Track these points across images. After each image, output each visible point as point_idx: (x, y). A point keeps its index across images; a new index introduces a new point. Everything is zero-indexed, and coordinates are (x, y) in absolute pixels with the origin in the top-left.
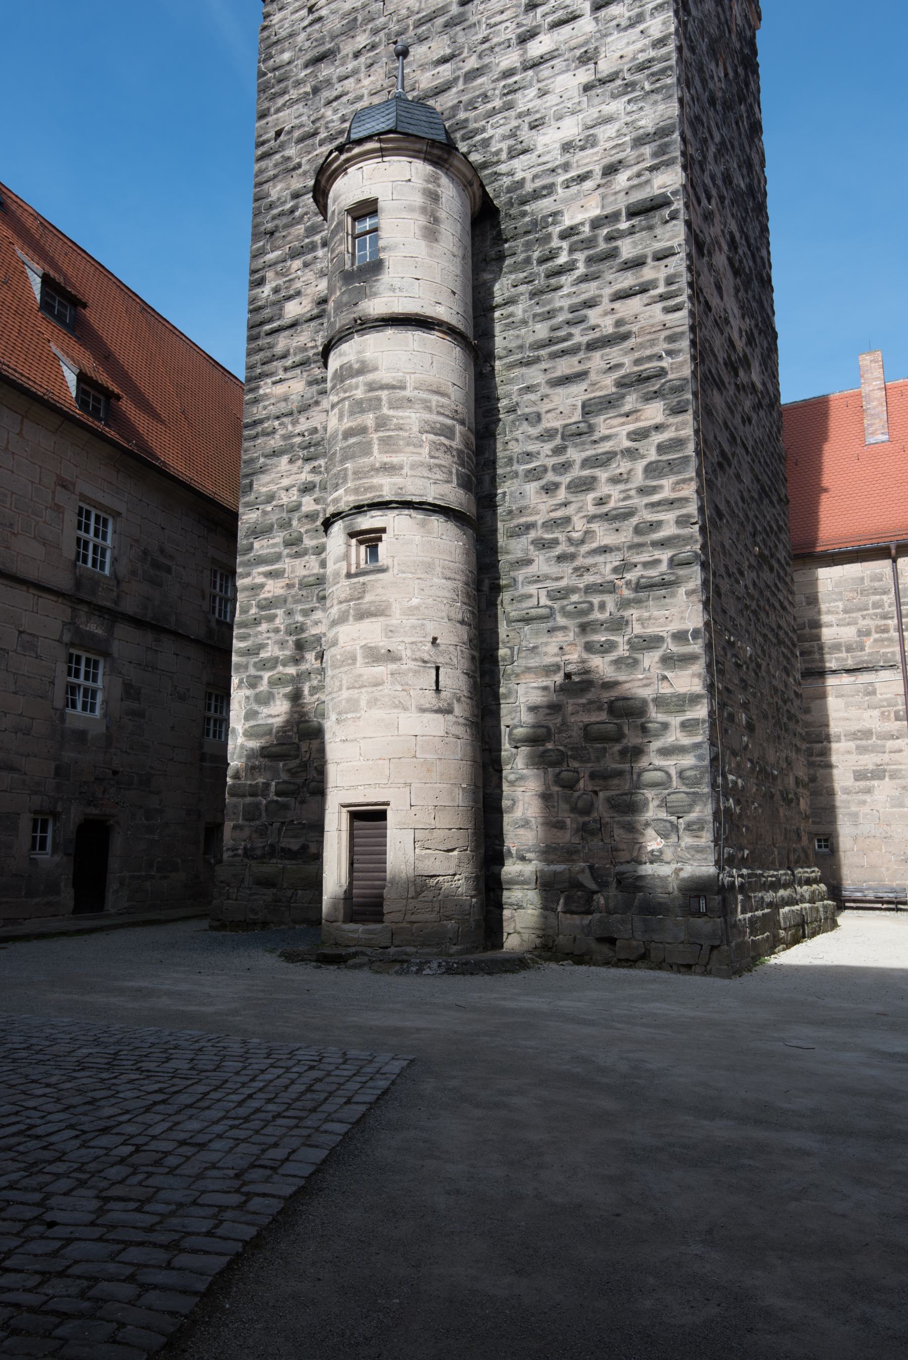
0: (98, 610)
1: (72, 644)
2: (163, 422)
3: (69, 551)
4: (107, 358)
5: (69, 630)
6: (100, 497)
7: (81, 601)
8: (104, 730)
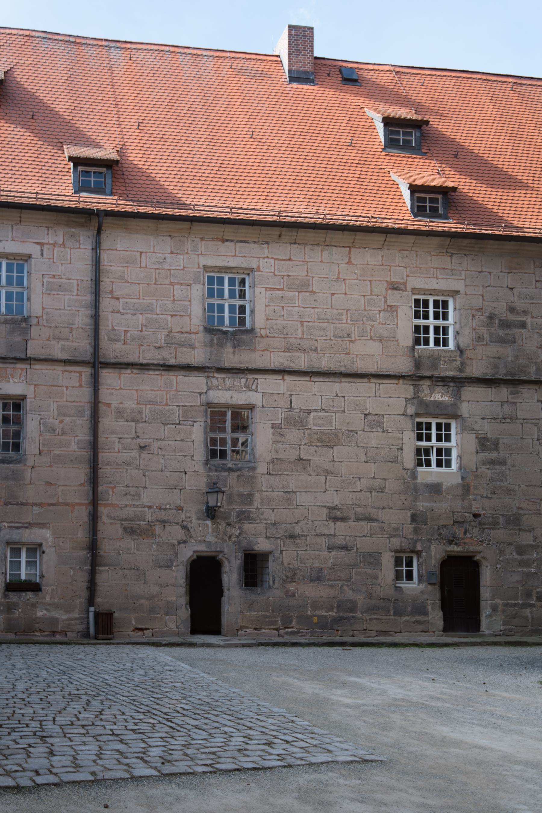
0: (444, 381)
1: (418, 415)
2: (526, 187)
3: (406, 337)
4: (456, 156)
5: (413, 404)
6: (434, 285)
7: (422, 378)
8: (459, 481)
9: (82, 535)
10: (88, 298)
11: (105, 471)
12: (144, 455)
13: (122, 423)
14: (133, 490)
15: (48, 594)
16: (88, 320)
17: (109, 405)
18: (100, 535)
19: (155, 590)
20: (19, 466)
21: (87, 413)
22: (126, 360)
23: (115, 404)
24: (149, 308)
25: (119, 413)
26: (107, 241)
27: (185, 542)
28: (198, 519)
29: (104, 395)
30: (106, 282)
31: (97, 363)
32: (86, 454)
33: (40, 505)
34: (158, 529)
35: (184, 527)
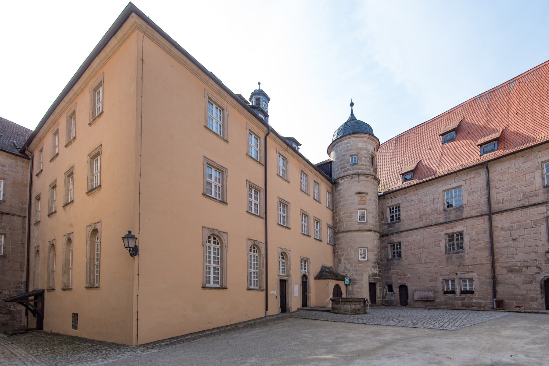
9: (489, 274)
10: (486, 192)
11: (497, 251)
12: (515, 242)
13: (504, 232)
14: (510, 256)
15: (476, 295)
16: (486, 200)
17: (497, 227)
18: (496, 274)
19: (525, 292)
20: (462, 254)
21: (488, 232)
22: (504, 209)
23: (500, 226)
24: (514, 187)
25: (502, 229)
26: (491, 170)
27: (539, 273)
28: (546, 263)
29: (495, 224)
30: (492, 184)
31: (490, 213)
32: (489, 246)
33: (471, 265)
34: (524, 269)
35: (538, 267)
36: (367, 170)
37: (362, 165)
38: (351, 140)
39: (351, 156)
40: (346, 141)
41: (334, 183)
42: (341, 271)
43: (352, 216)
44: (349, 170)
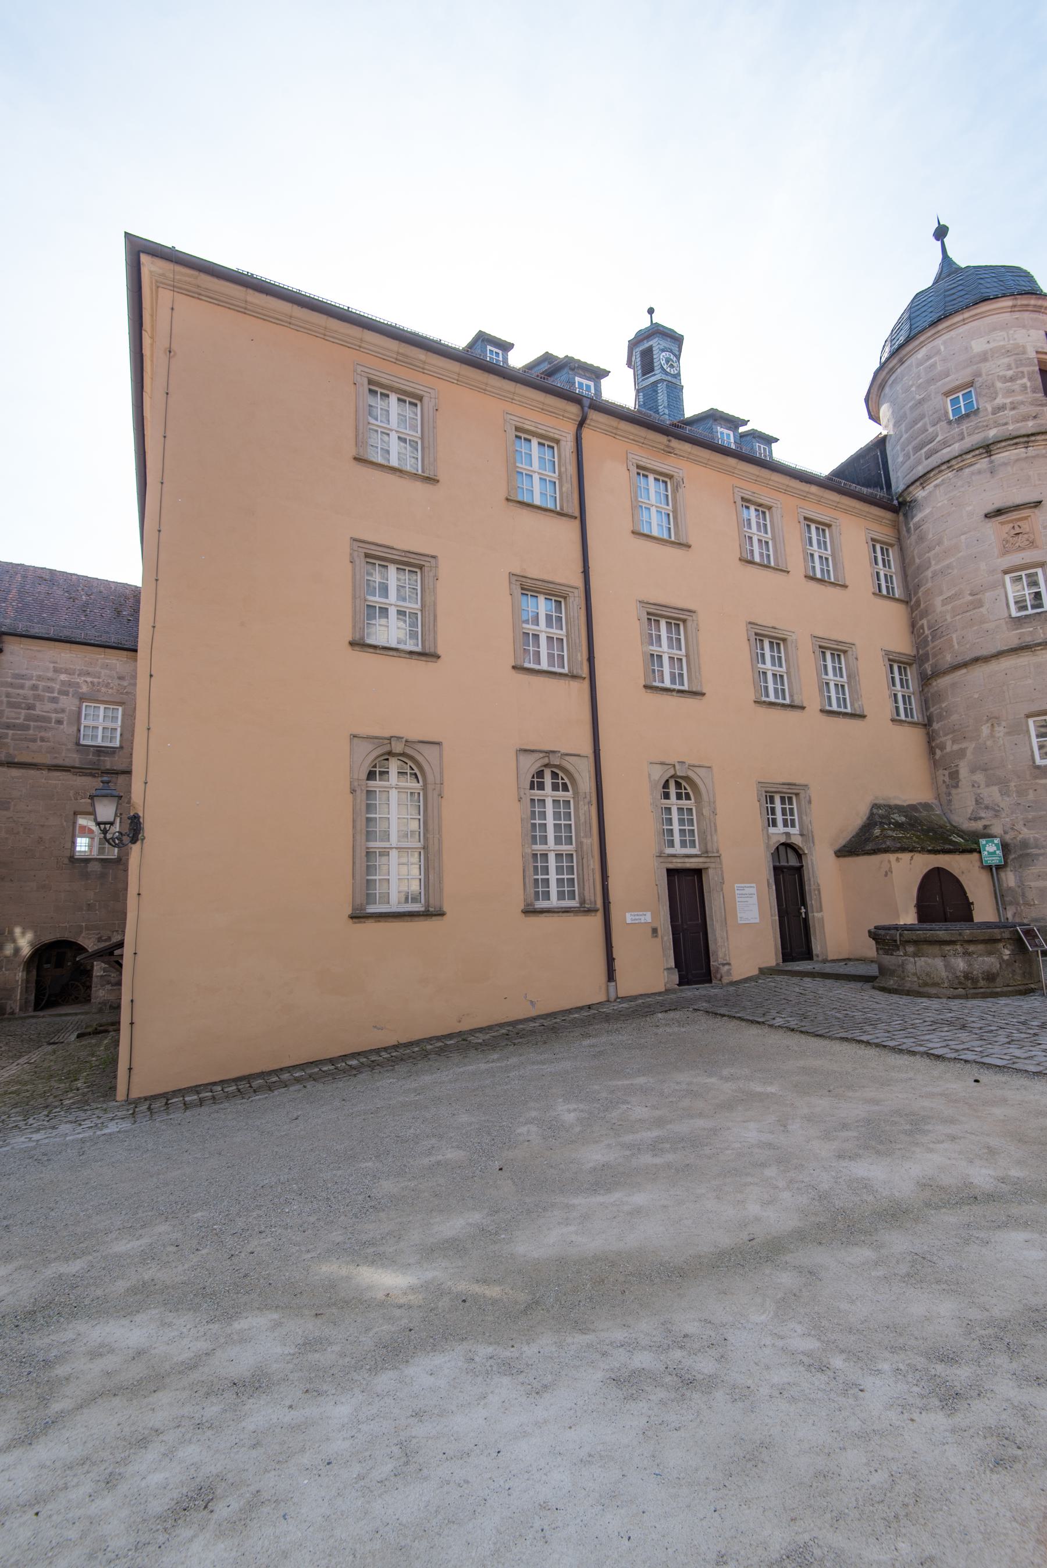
36: (1025, 419)
37: (1002, 408)
38: (939, 342)
39: (947, 394)
40: (921, 354)
41: (899, 507)
42: (962, 814)
43: (980, 604)
44: (945, 444)
